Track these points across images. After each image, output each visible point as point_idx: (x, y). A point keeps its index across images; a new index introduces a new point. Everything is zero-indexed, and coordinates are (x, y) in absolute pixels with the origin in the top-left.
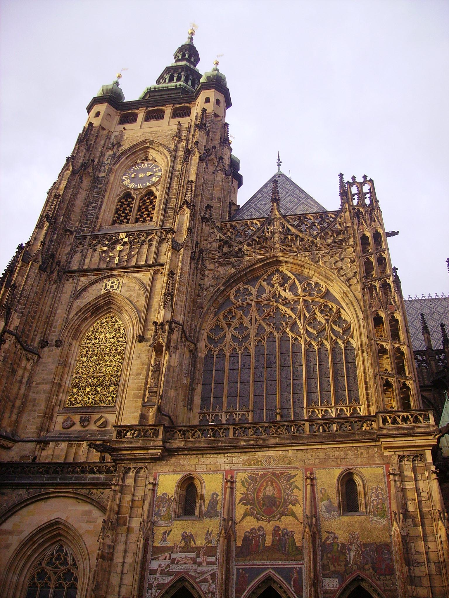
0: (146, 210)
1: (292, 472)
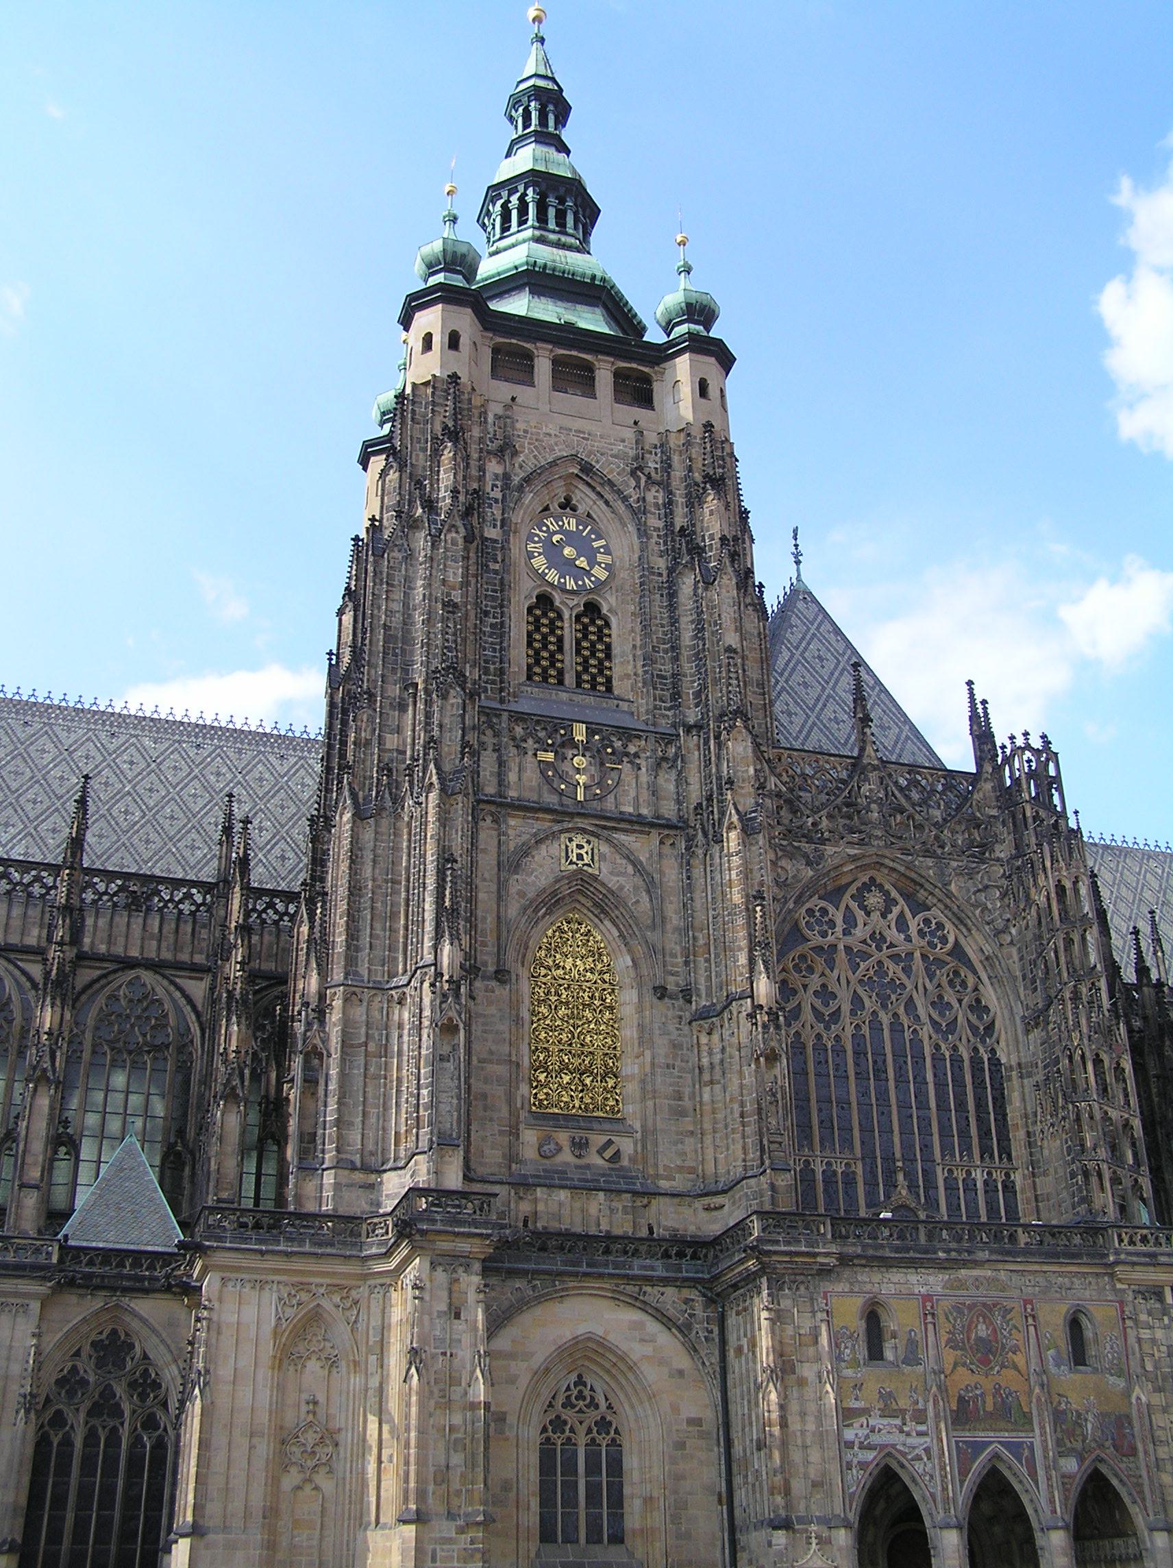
0: (593, 655)
1: (1008, 1304)
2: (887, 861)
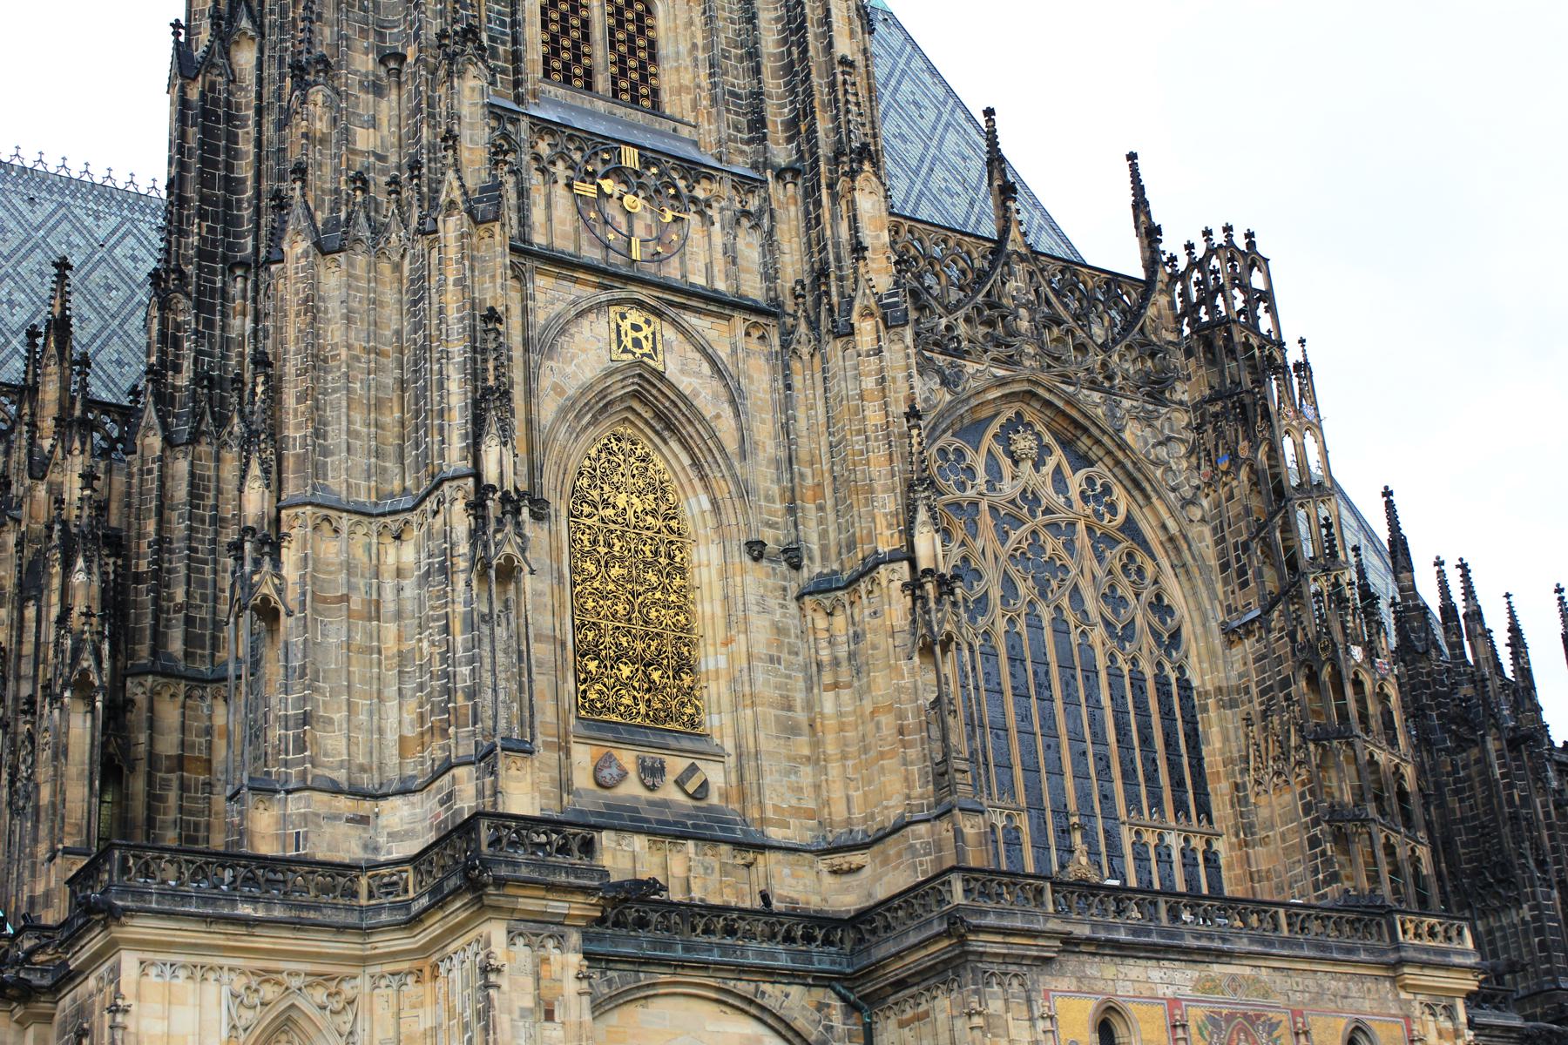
0: (632, 52)
1: (1274, 1015)
2: (1041, 391)
